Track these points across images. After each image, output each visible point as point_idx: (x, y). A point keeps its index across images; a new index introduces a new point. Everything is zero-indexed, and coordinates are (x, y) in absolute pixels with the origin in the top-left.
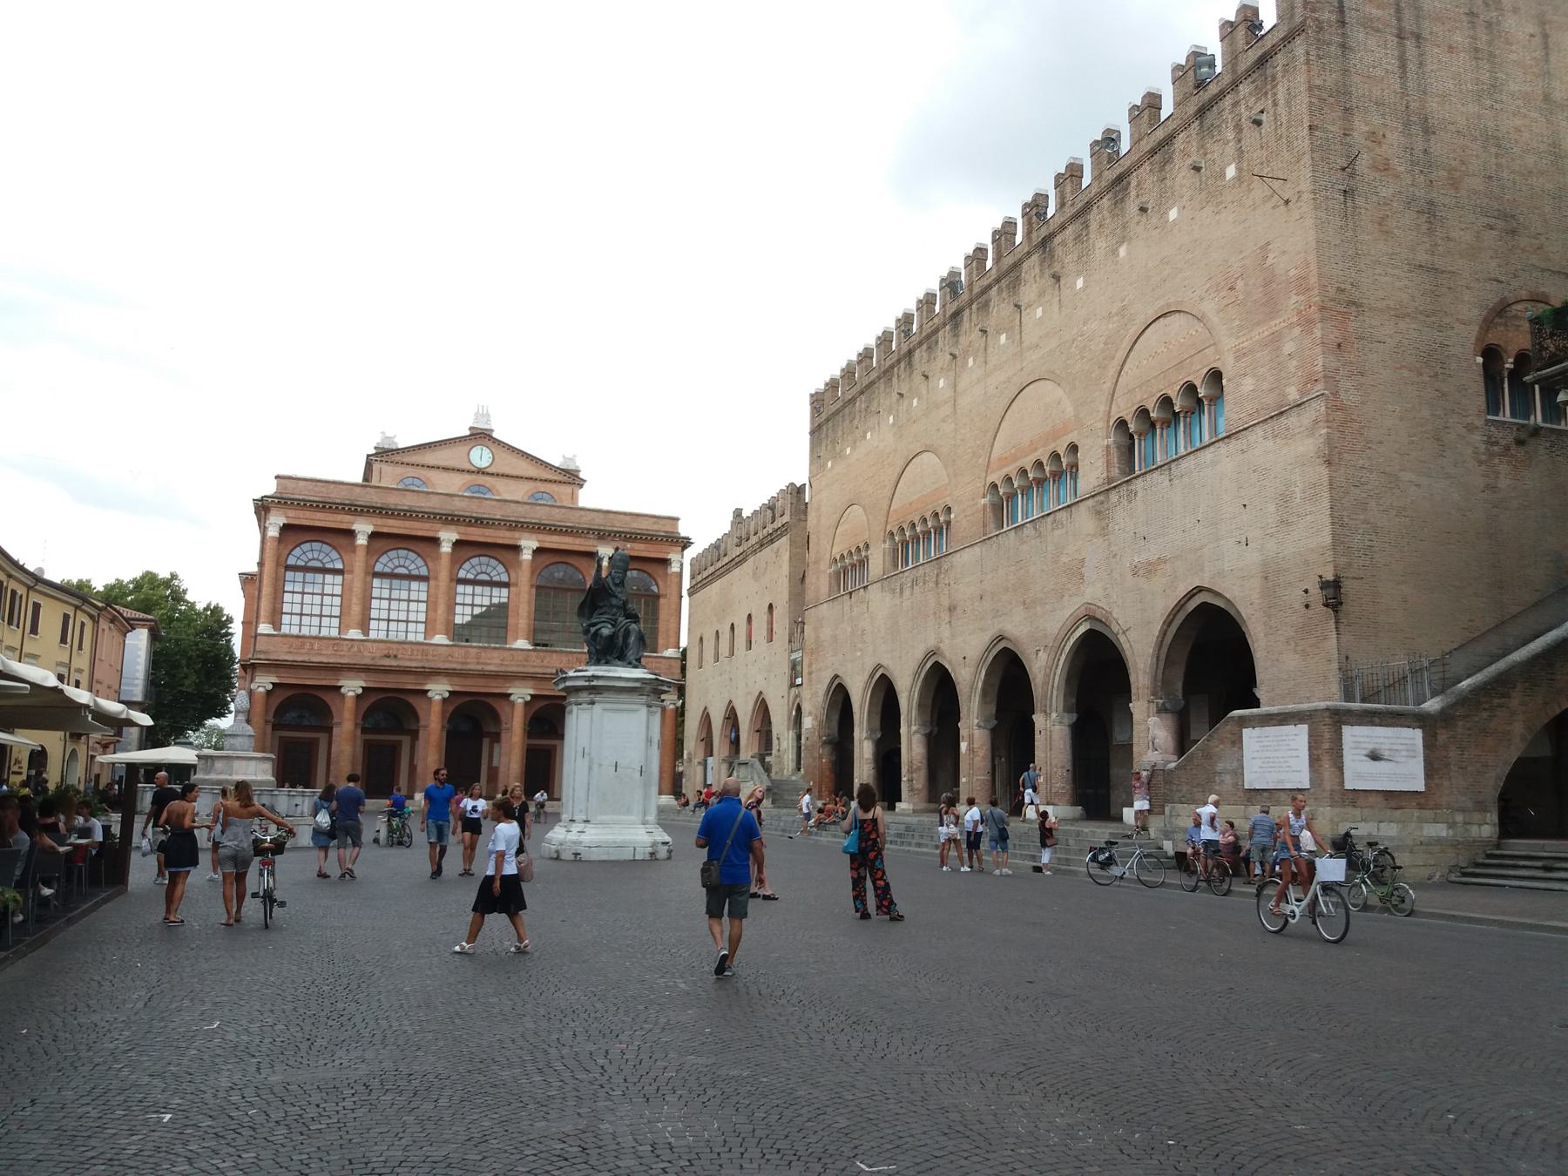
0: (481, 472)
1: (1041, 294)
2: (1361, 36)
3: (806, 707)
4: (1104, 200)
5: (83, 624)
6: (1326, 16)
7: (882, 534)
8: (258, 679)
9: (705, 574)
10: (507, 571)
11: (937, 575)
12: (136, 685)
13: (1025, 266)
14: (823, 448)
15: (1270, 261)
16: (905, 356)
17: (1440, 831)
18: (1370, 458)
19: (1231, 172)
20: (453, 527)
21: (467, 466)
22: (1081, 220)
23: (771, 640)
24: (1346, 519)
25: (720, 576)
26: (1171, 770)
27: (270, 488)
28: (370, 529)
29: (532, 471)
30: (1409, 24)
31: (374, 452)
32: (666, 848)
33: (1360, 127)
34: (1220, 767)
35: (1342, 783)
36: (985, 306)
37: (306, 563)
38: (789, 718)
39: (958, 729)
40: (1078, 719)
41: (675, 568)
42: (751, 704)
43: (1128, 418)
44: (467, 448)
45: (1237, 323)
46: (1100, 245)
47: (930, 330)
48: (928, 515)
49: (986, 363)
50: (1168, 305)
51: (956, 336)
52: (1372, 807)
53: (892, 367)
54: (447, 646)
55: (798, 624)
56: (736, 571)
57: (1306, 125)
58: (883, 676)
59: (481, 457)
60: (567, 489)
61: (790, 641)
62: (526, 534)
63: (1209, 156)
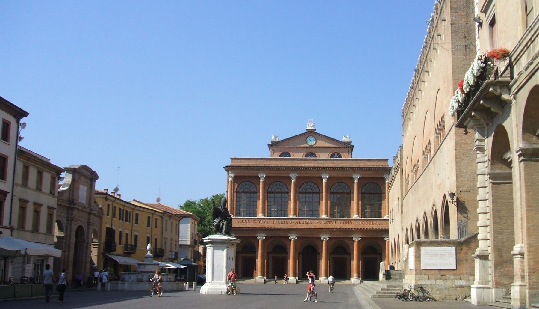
5: (156, 219)
12: (188, 239)
24: (462, 170)
27: (229, 163)
35: (420, 266)
44: (305, 139)
54: (295, 219)
59: (311, 142)
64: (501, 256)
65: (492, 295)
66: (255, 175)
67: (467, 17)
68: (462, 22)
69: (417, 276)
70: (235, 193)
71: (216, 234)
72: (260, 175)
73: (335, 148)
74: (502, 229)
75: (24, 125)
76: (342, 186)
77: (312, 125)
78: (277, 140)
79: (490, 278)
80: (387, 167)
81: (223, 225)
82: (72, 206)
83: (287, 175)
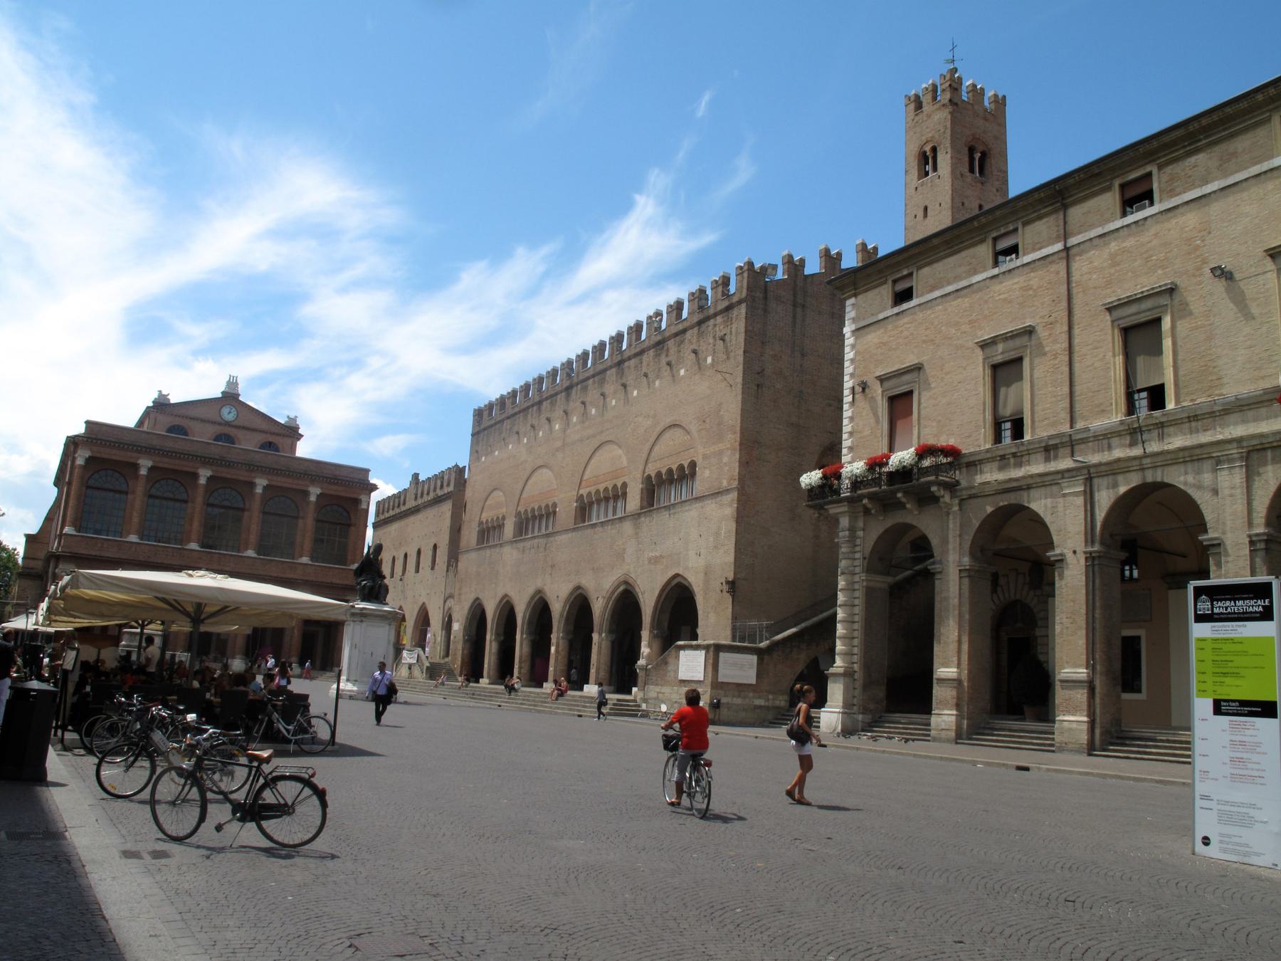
0: (228, 424)
1: (615, 392)
3: (455, 616)
8: (60, 566)
10: (243, 500)
13: (608, 372)
19: (709, 360)
21: (218, 419)
22: (639, 358)
23: (433, 568)
26: (650, 669)
27: (80, 429)
28: (150, 464)
29: (264, 426)
34: (670, 668)
36: (585, 389)
38: (443, 622)
39: (550, 639)
41: (364, 506)
47: (553, 392)
50: (676, 421)
51: (568, 400)
59: (228, 414)
60: (289, 441)
66: (132, 460)
72: (141, 462)
83: (192, 470)
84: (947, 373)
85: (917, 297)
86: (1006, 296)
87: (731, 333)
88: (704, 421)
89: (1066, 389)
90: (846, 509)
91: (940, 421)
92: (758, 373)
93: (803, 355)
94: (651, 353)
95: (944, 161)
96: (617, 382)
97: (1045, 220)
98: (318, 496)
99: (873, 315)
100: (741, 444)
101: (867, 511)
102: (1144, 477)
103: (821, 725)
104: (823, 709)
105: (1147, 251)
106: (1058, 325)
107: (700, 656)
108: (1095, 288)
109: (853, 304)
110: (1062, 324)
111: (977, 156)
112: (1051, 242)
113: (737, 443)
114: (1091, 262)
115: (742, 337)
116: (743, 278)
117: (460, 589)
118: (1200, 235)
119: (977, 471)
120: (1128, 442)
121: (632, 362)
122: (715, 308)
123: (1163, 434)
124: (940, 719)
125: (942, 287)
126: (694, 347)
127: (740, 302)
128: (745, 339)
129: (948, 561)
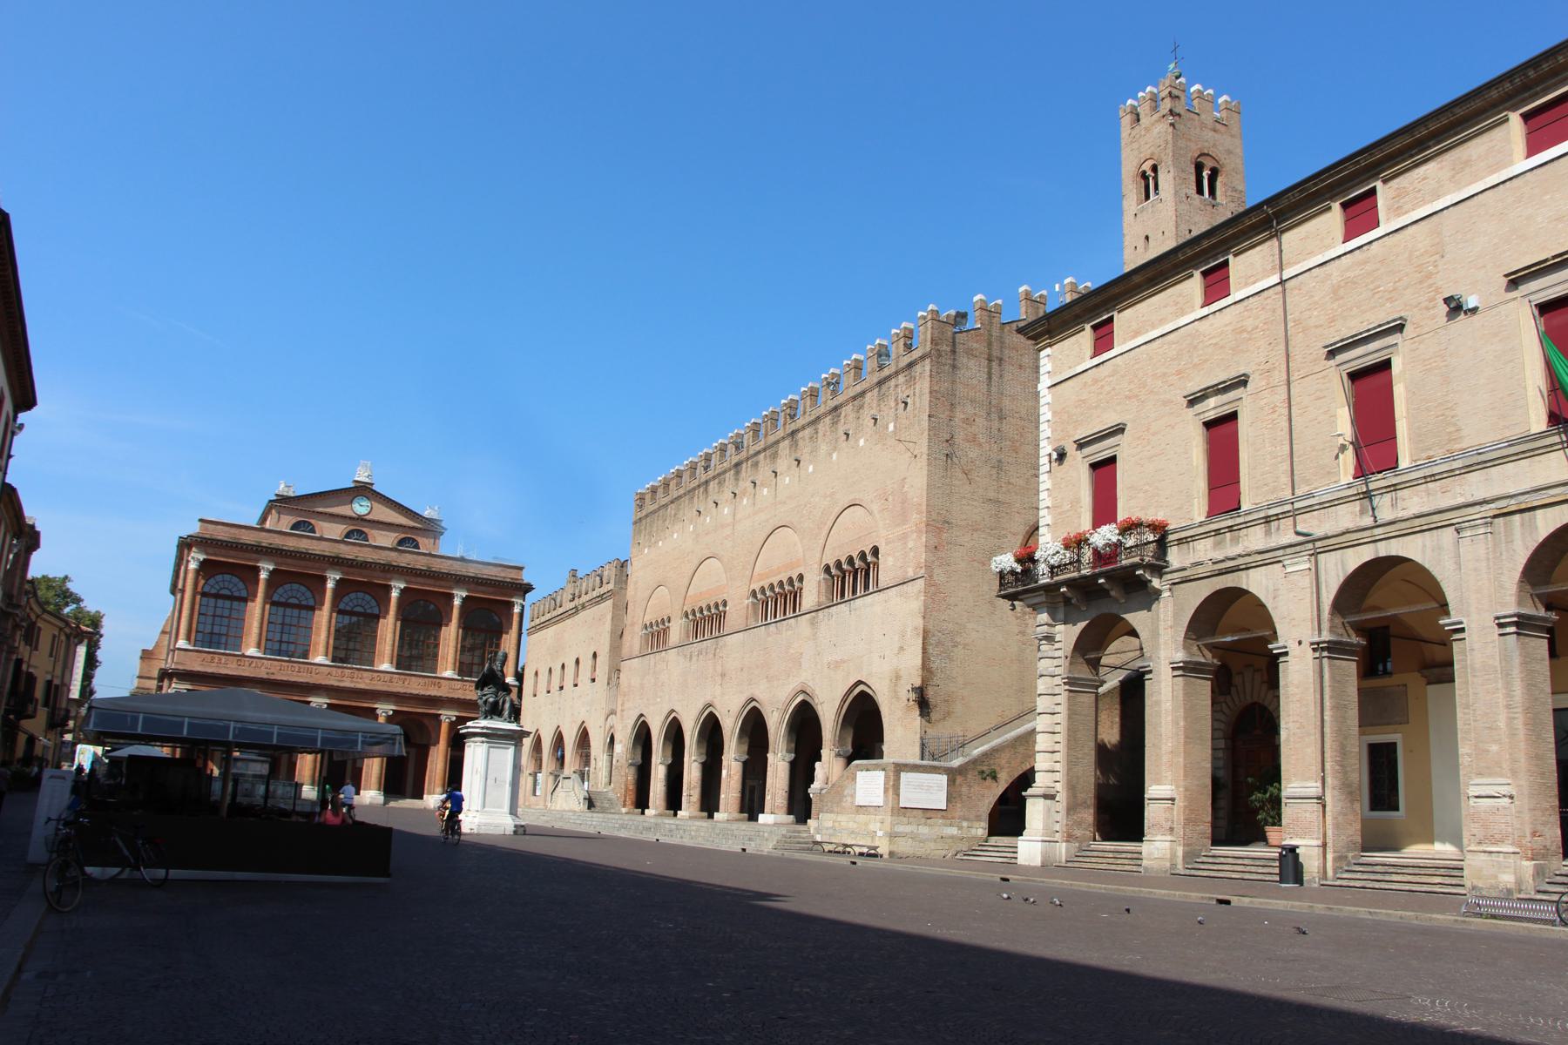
2: (965, 360)
4: (828, 418)
6: (945, 347)
7: (680, 613)
8: (173, 685)
9: (543, 619)
10: (378, 605)
11: (715, 649)
14: (642, 535)
15: (905, 489)
16: (703, 483)
17: (954, 831)
18: (949, 615)
20: (338, 567)
22: (814, 427)
25: (555, 623)
27: (194, 528)
30: (996, 353)
31: (275, 498)
32: (522, 829)
33: (959, 415)
34: (846, 793)
35: (899, 803)
36: (756, 465)
37: (218, 591)
39: (721, 760)
40: (795, 758)
41: (517, 610)
42: (576, 730)
43: (831, 565)
45: (888, 522)
46: (824, 448)
48: (712, 605)
49: (754, 504)
51: (737, 480)
52: (915, 817)
53: (694, 489)
55: (616, 670)
56: (568, 622)
57: (927, 414)
58: (675, 718)
59: (361, 507)
61: (608, 684)
62: (396, 576)
63: (882, 413)
64: (1075, 796)
65: (1060, 853)
67: (951, 411)
68: (944, 416)
69: (893, 818)
70: (199, 597)
71: (485, 718)
73: (409, 527)
74: (1078, 758)
75: (21, 427)
76: (351, 600)
77: (366, 474)
78: (291, 494)
79: (1057, 827)
80: (520, 582)
81: (504, 702)
82: (10, 610)
84: (1154, 434)
85: (1119, 345)
86: (1218, 339)
87: (914, 395)
88: (886, 500)
89: (1287, 448)
90: (1043, 599)
91: (1146, 491)
92: (947, 441)
93: (1001, 418)
94: (828, 420)
95: (1166, 180)
96: (790, 456)
97: (1258, 248)
98: (463, 599)
99: (1070, 368)
100: (927, 525)
101: (1067, 601)
102: (1377, 551)
103: (1019, 855)
104: (1020, 838)
105: (1372, 282)
106: (1277, 372)
107: (880, 776)
108: (1316, 327)
109: (1048, 356)
110: (1280, 371)
111: (1206, 174)
112: (1266, 275)
113: (923, 524)
114: (1312, 296)
115: (927, 397)
116: (927, 328)
117: (622, 705)
118: (1433, 259)
119: (1189, 549)
120: (1358, 509)
121: (807, 432)
122: (897, 366)
123: (1396, 499)
124: (1152, 847)
125: (1147, 331)
126: (873, 412)
127: (922, 358)
128: (930, 401)
129: (1159, 658)
